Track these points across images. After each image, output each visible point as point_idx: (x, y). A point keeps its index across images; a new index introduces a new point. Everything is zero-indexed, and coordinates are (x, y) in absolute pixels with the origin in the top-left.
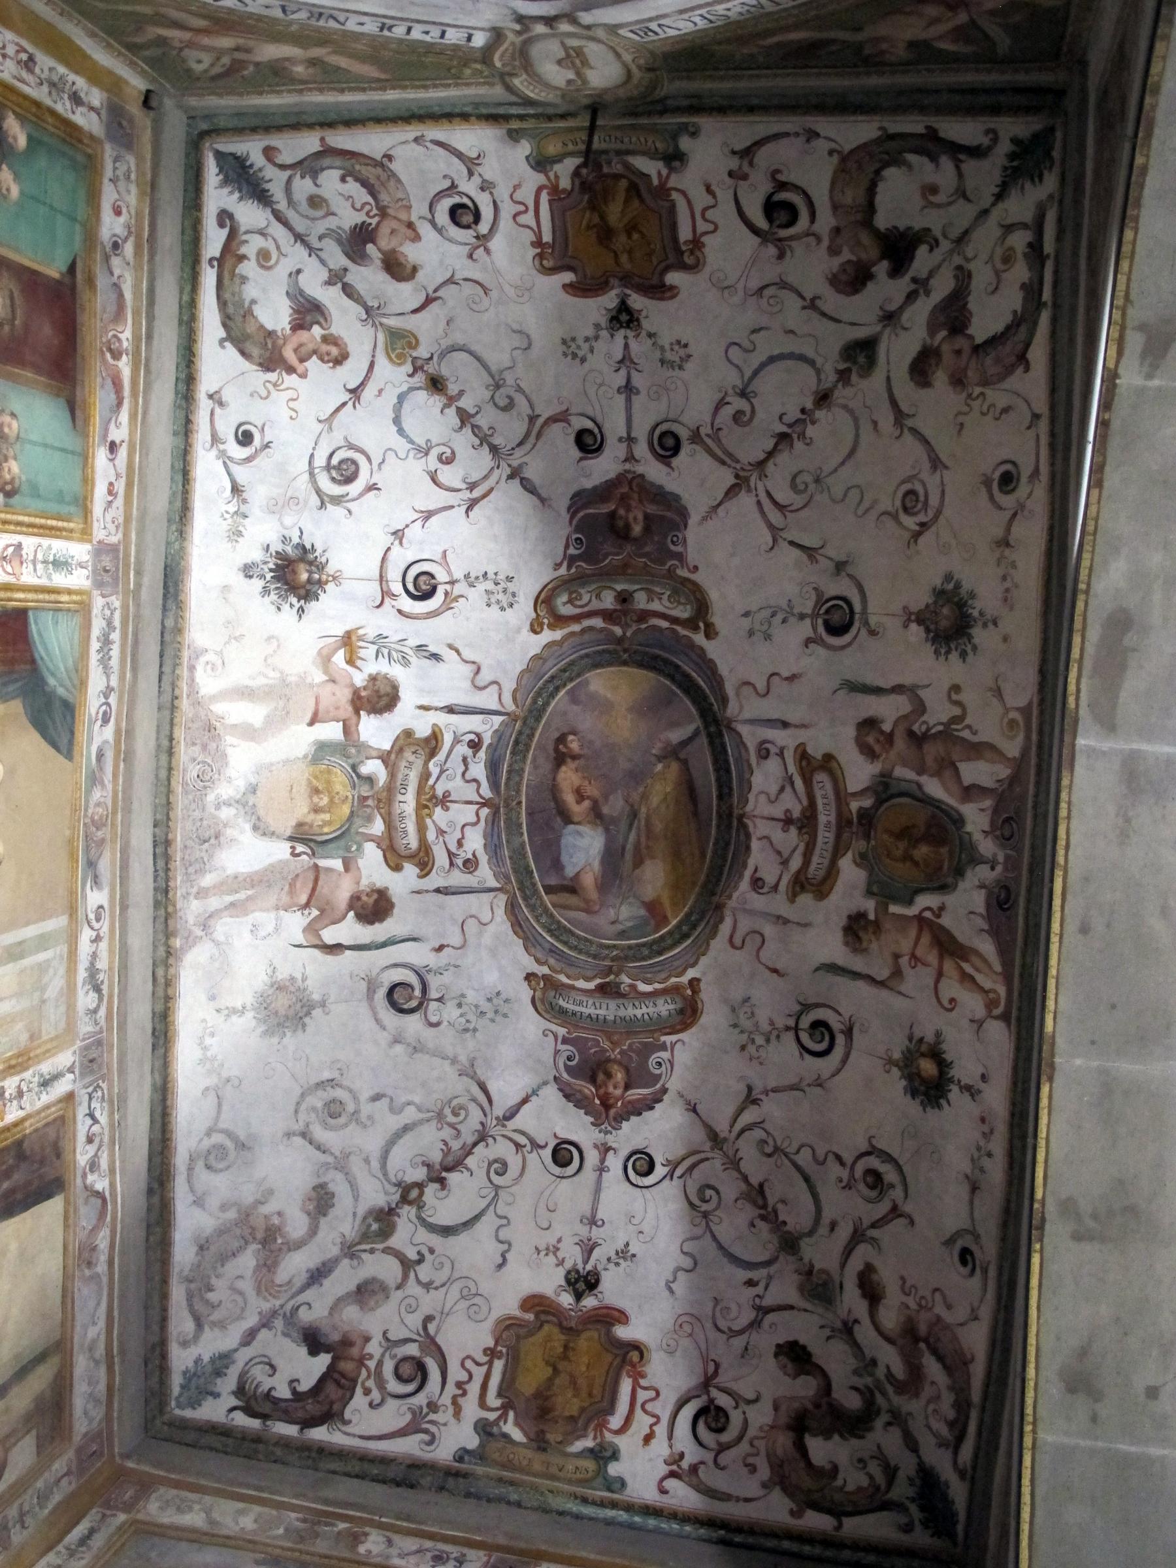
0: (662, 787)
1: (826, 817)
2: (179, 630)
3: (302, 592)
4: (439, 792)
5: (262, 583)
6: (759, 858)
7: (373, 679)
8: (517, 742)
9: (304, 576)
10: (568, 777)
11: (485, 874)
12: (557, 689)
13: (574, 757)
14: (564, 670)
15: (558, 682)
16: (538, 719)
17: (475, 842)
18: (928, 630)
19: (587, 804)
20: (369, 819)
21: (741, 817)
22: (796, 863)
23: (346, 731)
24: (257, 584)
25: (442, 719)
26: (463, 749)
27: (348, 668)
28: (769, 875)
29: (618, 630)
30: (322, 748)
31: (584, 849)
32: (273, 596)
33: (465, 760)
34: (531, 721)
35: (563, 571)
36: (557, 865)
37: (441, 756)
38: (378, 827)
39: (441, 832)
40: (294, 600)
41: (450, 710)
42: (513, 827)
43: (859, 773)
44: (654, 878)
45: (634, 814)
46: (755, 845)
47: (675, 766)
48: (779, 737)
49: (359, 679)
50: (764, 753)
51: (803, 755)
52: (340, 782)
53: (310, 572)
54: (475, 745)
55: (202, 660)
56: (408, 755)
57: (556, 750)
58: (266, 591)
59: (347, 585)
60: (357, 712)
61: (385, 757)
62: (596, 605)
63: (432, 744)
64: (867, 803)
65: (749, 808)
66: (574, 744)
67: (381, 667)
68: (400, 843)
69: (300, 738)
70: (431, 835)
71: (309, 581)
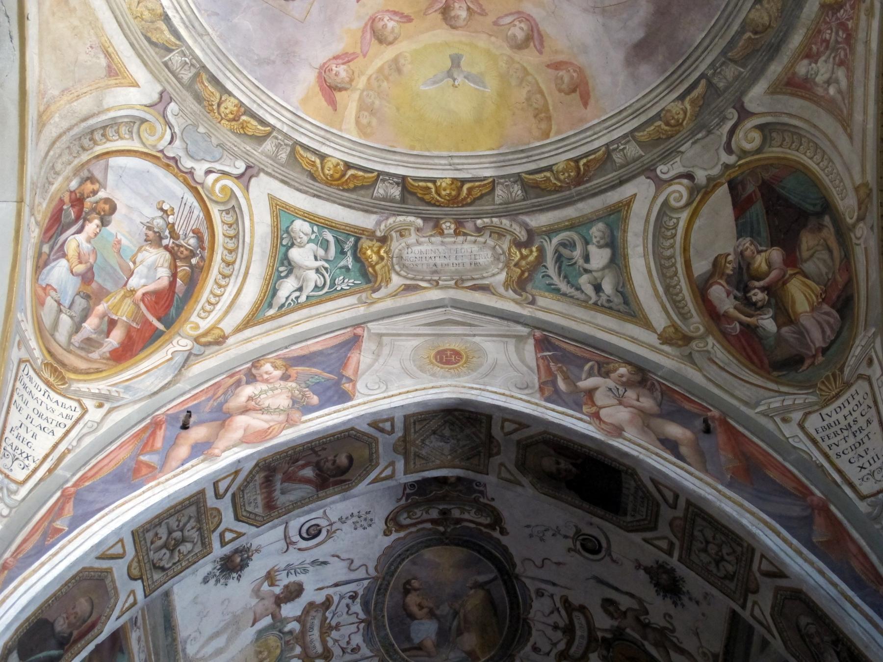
0: (474, 601)
1: (581, 632)
2: (174, 640)
3: (239, 568)
4: (333, 623)
5: (215, 579)
6: (535, 637)
7: (286, 587)
8: (379, 589)
9: (238, 560)
10: (412, 600)
11: (365, 651)
12: (403, 560)
13: (416, 590)
14: (407, 550)
15: (402, 557)
16: (392, 576)
17: (357, 640)
18: (651, 578)
19: (425, 610)
20: (293, 649)
21: (525, 620)
22: (562, 646)
23: (274, 617)
24: (212, 581)
25: (330, 591)
26: (347, 601)
27: (271, 588)
28: (545, 647)
29: (441, 529)
30: (260, 633)
31: (425, 630)
32: (222, 581)
33: (348, 606)
34: (388, 578)
35: (403, 502)
36: (409, 639)
37: (333, 608)
38: (298, 650)
39: (336, 641)
40: (235, 575)
41: (336, 585)
42: (380, 627)
43: (603, 622)
44: (470, 641)
45: (456, 614)
46: (534, 632)
47: (481, 593)
48: (551, 589)
49: (277, 590)
50: (540, 593)
51: (566, 601)
52: (273, 640)
53: (241, 556)
54: (353, 598)
55: (189, 641)
56: (313, 613)
57: (405, 588)
58: (218, 581)
59: (264, 551)
60: (279, 606)
61: (298, 619)
62: (425, 516)
63: (328, 603)
64: (609, 636)
65: (531, 616)
66: (415, 584)
67: (293, 578)
68: (312, 653)
69: (249, 634)
70: (330, 643)
71: (242, 560)
